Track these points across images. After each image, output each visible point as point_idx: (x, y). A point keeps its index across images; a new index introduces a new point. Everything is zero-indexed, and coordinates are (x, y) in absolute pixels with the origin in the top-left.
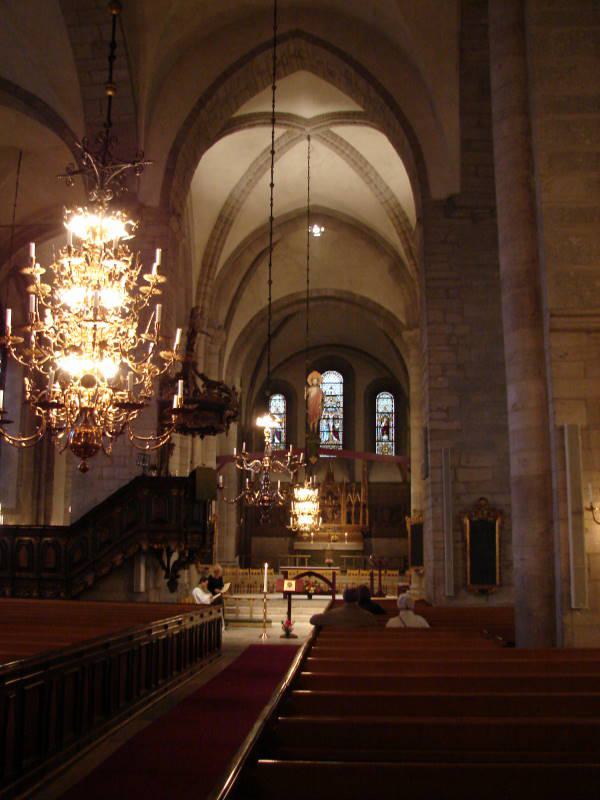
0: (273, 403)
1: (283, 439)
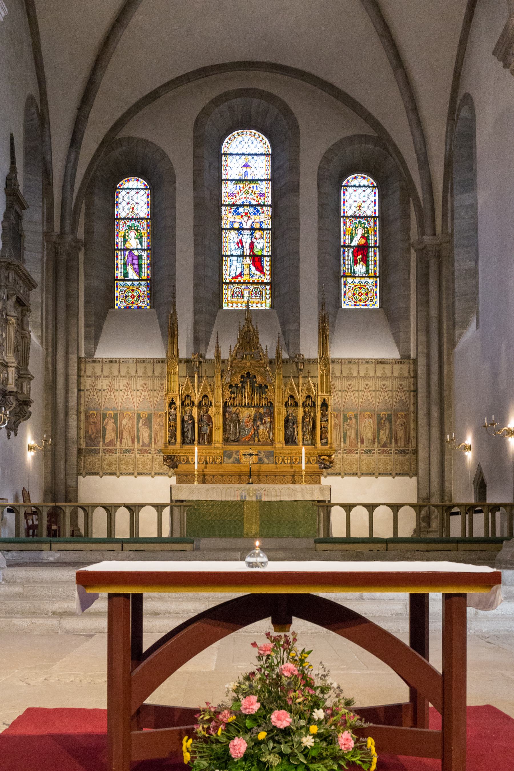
0: (122, 197)
1: (146, 272)
